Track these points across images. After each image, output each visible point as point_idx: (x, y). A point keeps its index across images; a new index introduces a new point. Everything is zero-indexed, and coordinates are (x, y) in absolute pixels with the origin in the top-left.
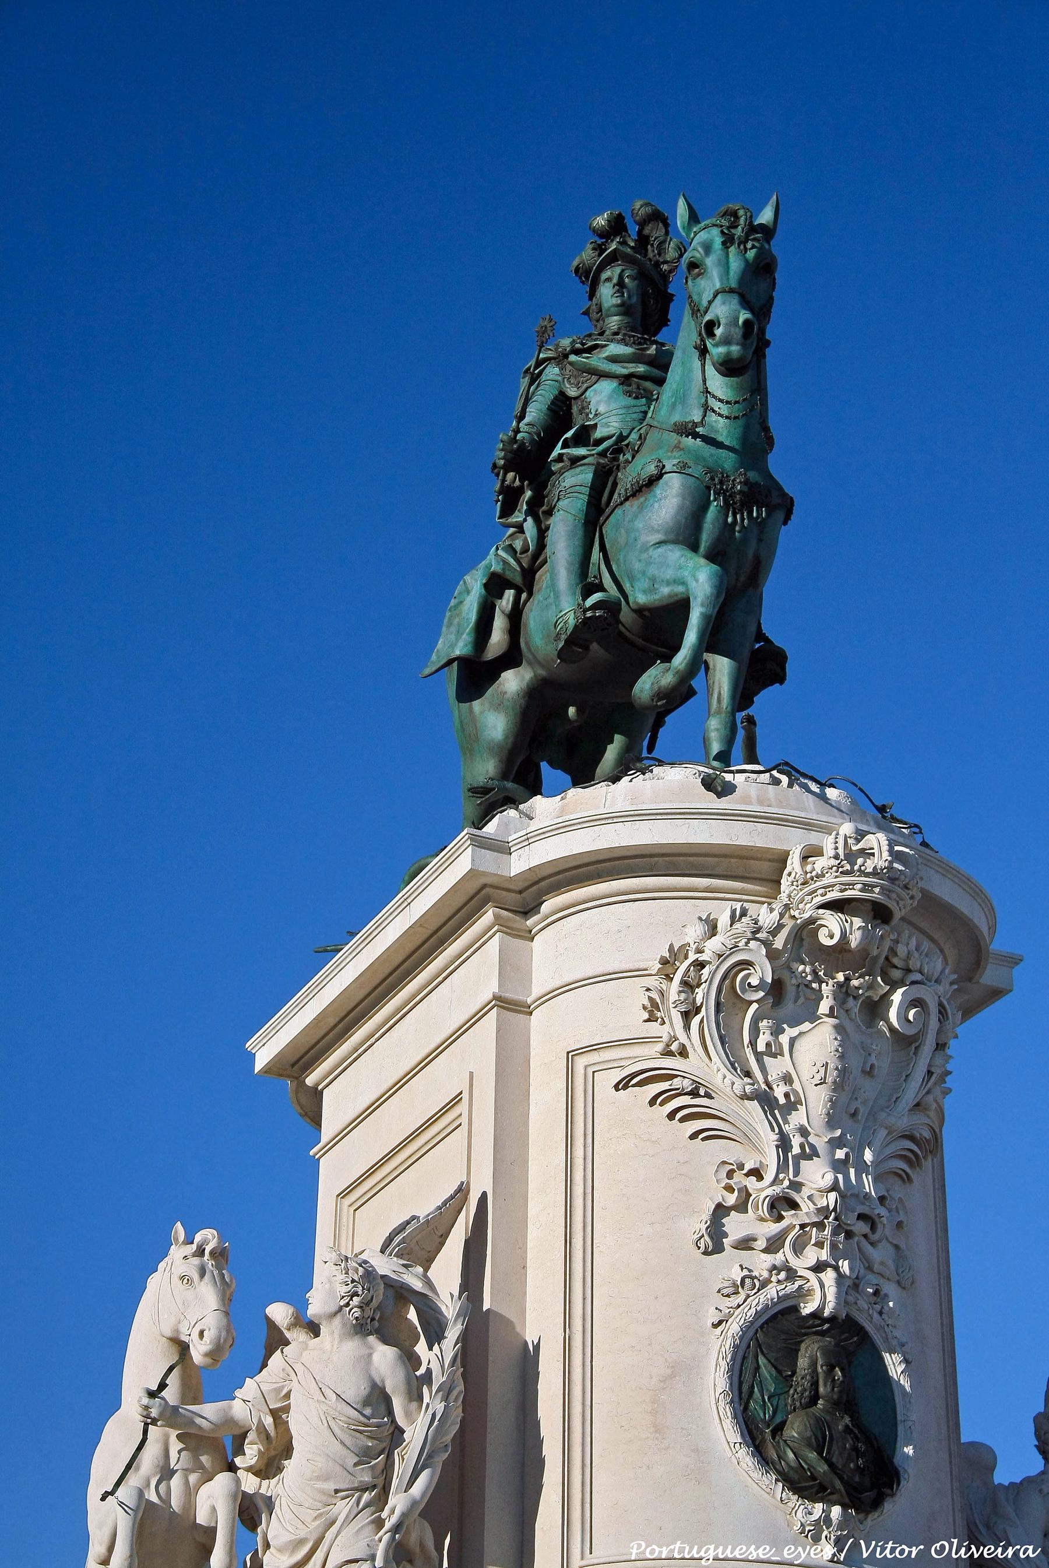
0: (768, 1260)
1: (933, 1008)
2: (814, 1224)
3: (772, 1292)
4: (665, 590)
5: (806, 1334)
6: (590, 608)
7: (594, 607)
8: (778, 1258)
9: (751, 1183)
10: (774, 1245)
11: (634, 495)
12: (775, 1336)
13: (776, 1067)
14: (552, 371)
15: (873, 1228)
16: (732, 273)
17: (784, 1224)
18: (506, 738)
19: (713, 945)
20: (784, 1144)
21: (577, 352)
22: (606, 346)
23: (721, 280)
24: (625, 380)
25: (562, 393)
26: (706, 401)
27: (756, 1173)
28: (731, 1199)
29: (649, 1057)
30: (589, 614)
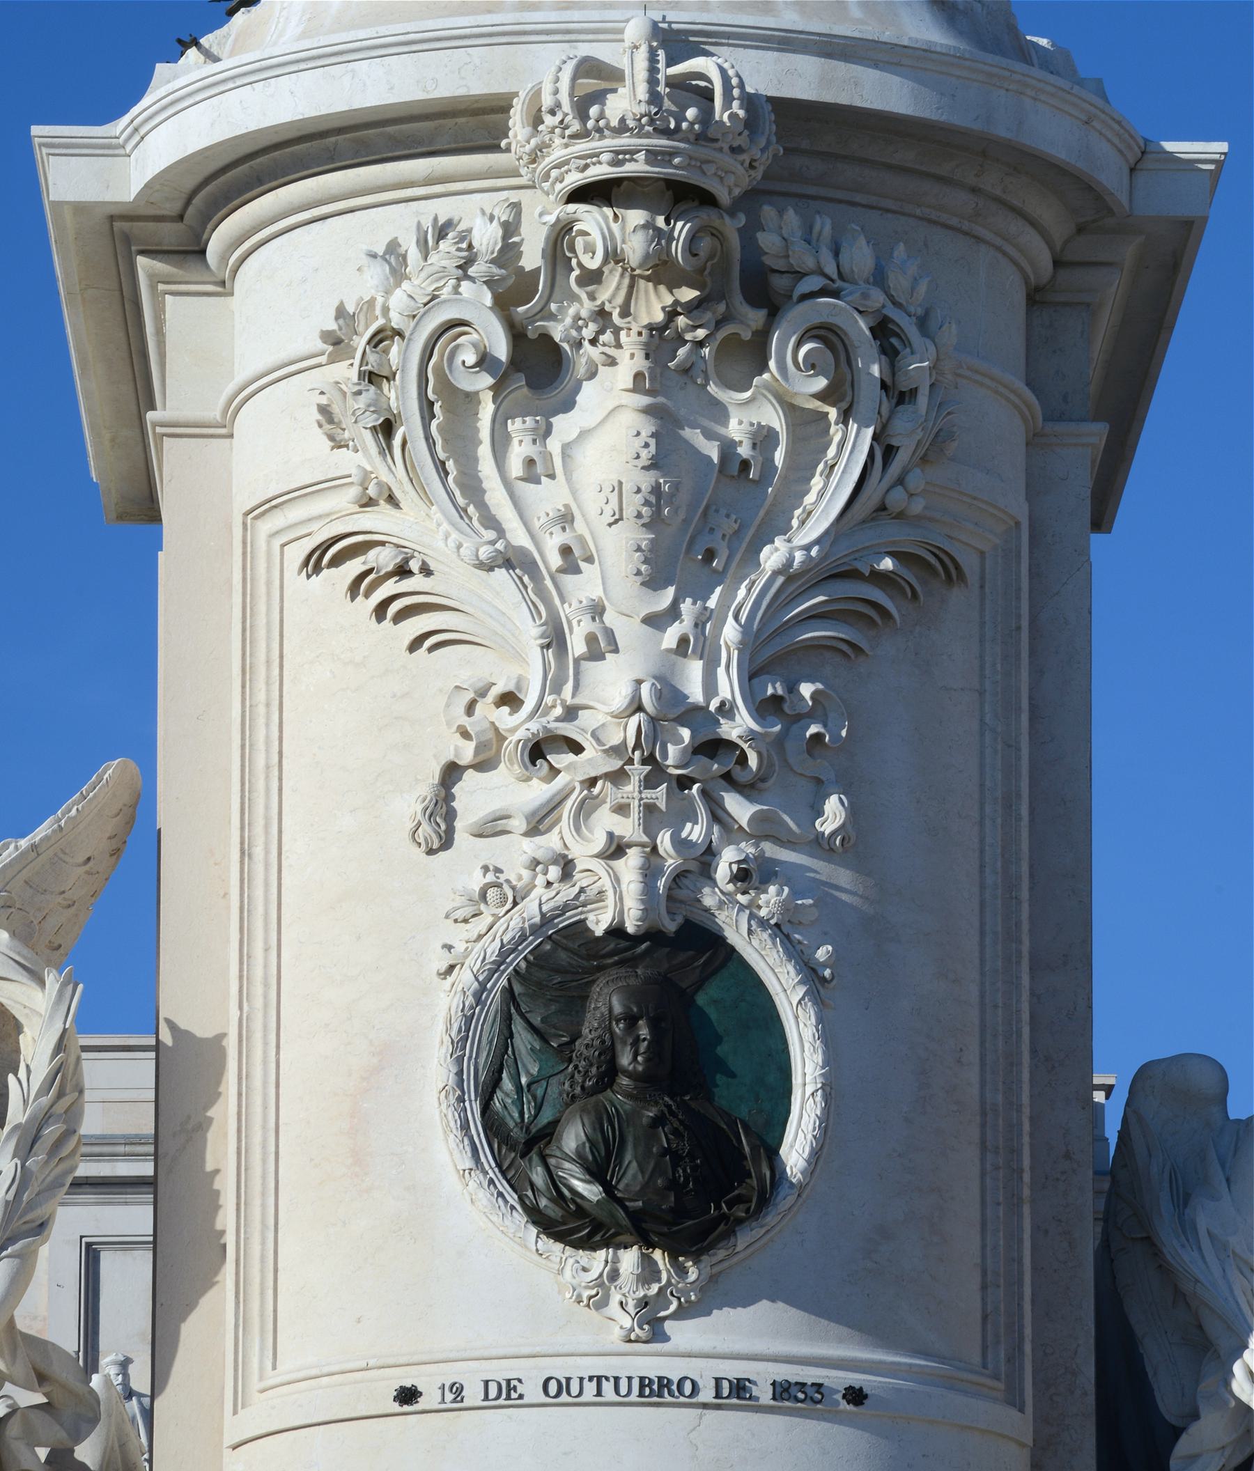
0: (532, 847)
2: (609, 776)
5: (600, 968)
8: (551, 842)
10: (539, 823)
12: (551, 976)
13: (547, 497)
19: (399, 302)
20: (555, 639)
27: (510, 700)
28: (467, 752)
29: (336, 514)
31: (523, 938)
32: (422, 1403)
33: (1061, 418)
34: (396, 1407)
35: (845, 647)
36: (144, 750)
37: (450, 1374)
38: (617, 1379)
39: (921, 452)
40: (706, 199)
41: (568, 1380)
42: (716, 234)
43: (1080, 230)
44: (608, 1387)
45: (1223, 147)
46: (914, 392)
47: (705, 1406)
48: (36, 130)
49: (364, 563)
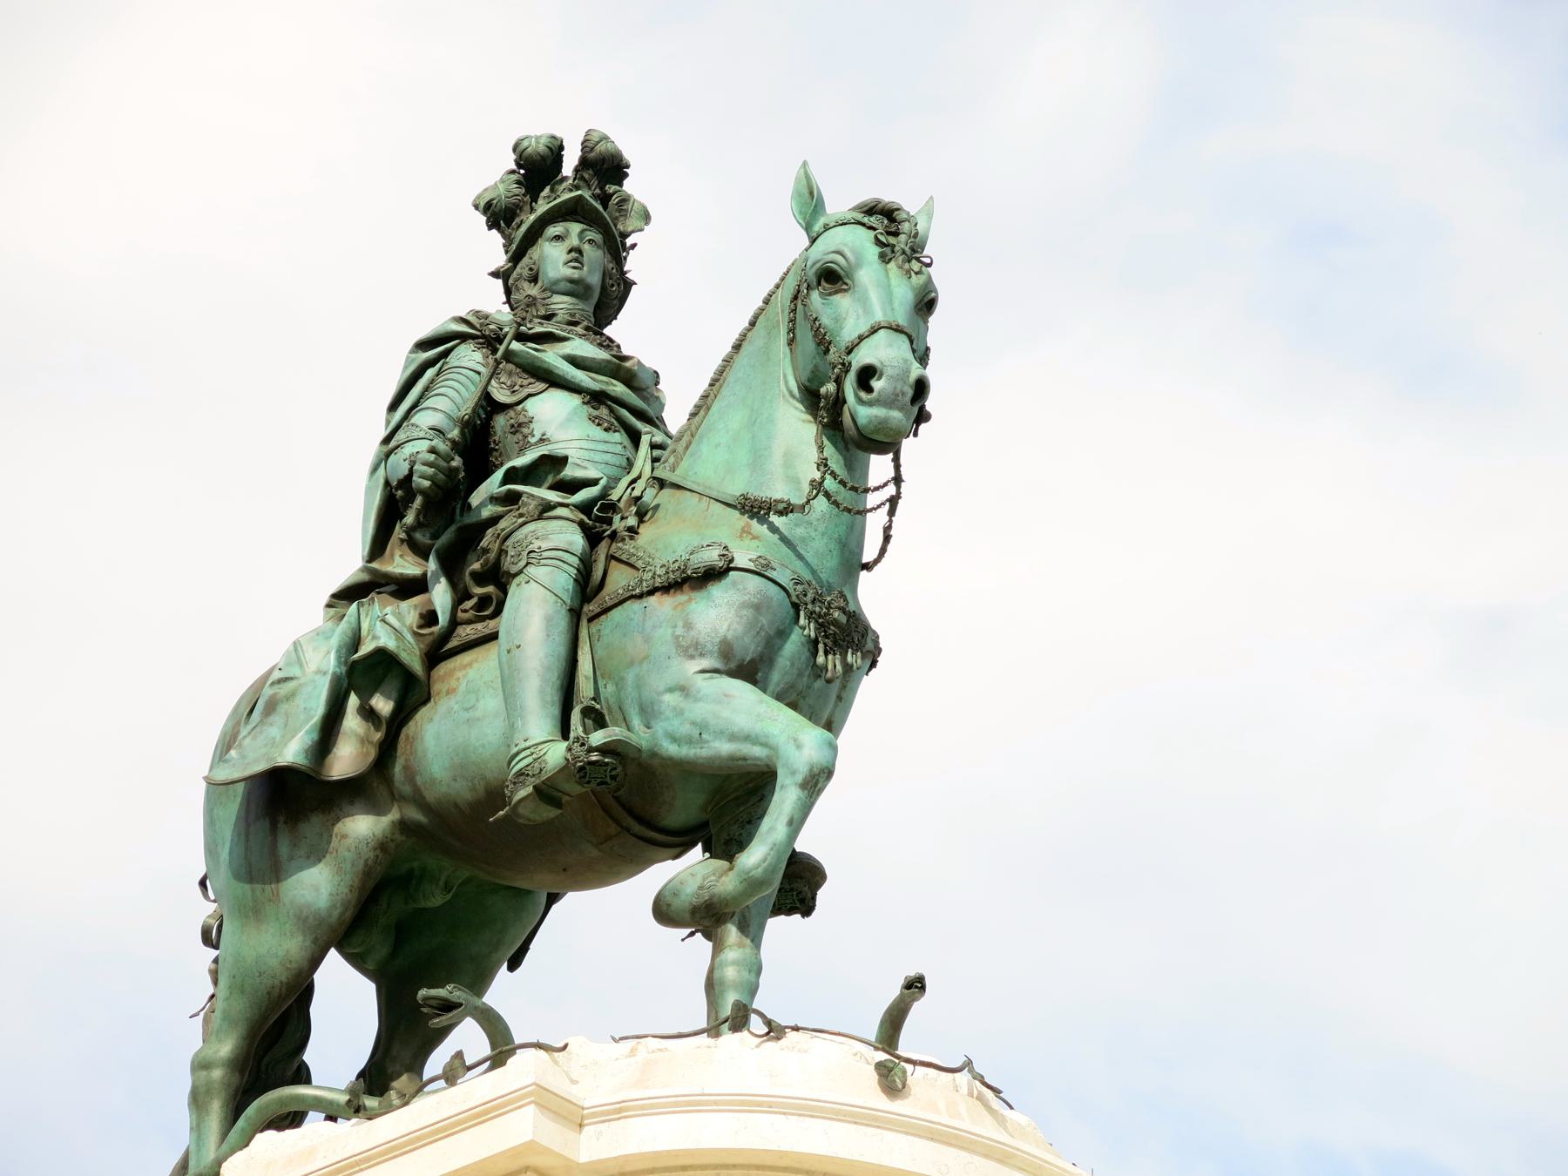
4: (724, 748)
6: (597, 749)
7: (604, 750)
11: (668, 588)
14: (469, 357)
16: (896, 305)
18: (334, 906)
21: (520, 337)
22: (565, 339)
23: (883, 309)
24: (597, 398)
25: (486, 396)
26: (823, 479)
30: (594, 757)
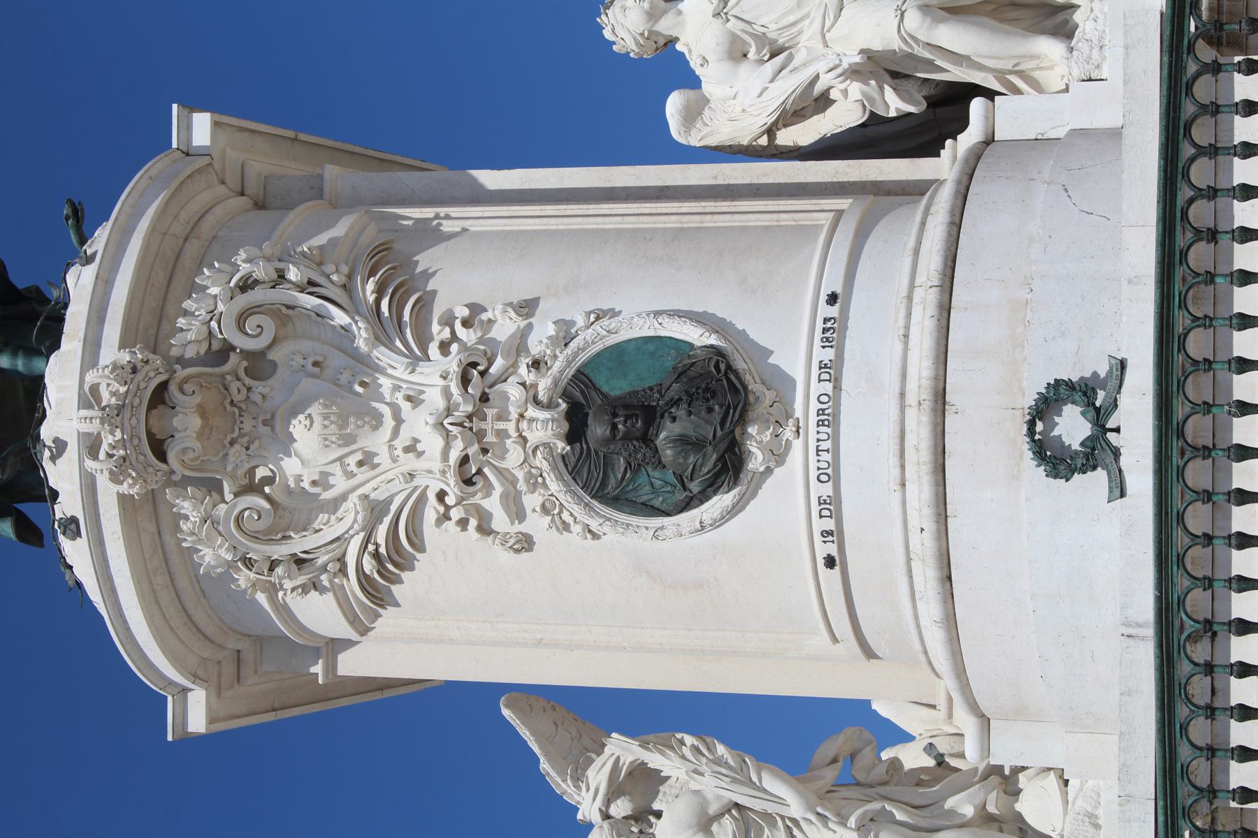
1: (243, 300)
3: (554, 486)
9: (450, 500)
15: (474, 365)
17: (486, 470)
27: (441, 496)
28: (473, 523)
31: (571, 491)
32: (835, 553)
33: (321, 190)
34: (837, 568)
35: (417, 307)
36: (488, 694)
37: (818, 538)
38: (818, 440)
39: (314, 266)
40: (163, 386)
41: (819, 469)
42: (186, 380)
43: (223, 182)
44: (824, 445)
45: (175, 106)
46: (278, 270)
47: (837, 388)
48: (170, 738)
49: (534, 510)
